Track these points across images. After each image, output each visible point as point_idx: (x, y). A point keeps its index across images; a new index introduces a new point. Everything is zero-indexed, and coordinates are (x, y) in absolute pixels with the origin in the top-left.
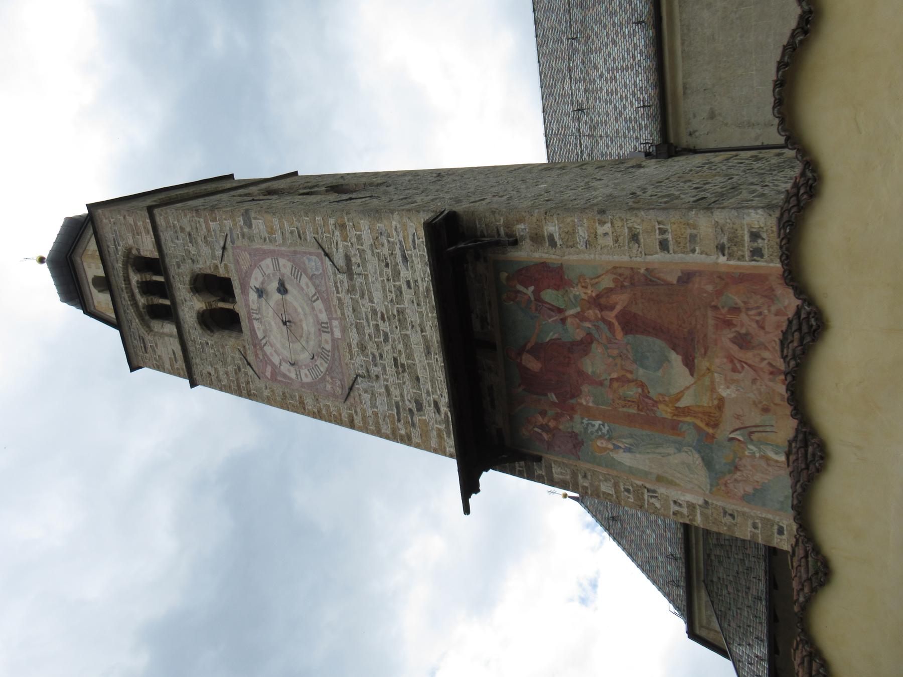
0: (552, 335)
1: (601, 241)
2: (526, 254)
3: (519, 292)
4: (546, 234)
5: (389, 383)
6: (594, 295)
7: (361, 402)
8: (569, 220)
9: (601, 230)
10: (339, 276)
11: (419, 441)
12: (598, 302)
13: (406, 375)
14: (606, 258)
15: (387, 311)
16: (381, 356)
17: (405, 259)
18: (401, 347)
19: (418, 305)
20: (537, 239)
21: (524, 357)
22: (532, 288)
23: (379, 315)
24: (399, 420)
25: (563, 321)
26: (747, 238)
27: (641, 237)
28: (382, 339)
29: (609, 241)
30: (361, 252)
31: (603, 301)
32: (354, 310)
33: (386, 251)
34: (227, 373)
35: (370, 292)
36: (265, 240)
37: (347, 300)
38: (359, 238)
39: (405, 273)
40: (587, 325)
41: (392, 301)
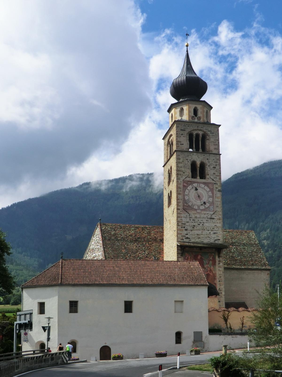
0: (205, 262)
1: (220, 272)
2: (217, 259)
3: (211, 257)
4: (220, 263)
5: (189, 223)
6: (212, 270)
7: (184, 214)
8: (223, 267)
9: (221, 272)
10: (210, 215)
11: (178, 228)
12: (211, 270)
13: (192, 228)
14: (217, 272)
15: (204, 226)
16: (195, 222)
17: (214, 233)
18: (198, 228)
19: (206, 234)
20: (219, 261)
21: (200, 256)
22: (212, 259)
23: (203, 224)
24: (182, 224)
25: (207, 264)
26: (221, 292)
27: (220, 278)
28: (198, 223)
29: (220, 273)
30: (215, 223)
31: (211, 271)
32: (203, 217)
33: (216, 229)
34: (181, 167)
35: (208, 223)
36: (216, 195)
37: (205, 216)
38: (217, 223)
39: (212, 232)
40: (207, 268)
41: (206, 228)
